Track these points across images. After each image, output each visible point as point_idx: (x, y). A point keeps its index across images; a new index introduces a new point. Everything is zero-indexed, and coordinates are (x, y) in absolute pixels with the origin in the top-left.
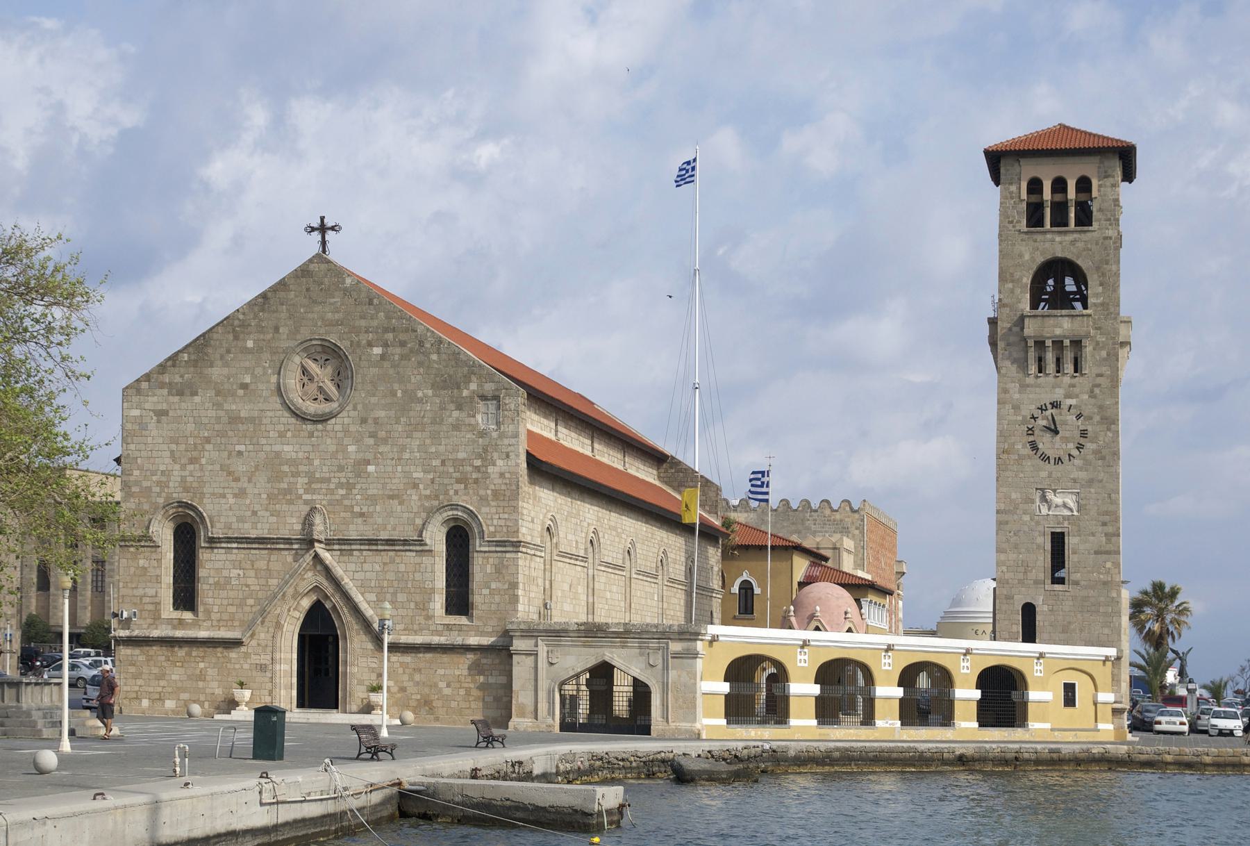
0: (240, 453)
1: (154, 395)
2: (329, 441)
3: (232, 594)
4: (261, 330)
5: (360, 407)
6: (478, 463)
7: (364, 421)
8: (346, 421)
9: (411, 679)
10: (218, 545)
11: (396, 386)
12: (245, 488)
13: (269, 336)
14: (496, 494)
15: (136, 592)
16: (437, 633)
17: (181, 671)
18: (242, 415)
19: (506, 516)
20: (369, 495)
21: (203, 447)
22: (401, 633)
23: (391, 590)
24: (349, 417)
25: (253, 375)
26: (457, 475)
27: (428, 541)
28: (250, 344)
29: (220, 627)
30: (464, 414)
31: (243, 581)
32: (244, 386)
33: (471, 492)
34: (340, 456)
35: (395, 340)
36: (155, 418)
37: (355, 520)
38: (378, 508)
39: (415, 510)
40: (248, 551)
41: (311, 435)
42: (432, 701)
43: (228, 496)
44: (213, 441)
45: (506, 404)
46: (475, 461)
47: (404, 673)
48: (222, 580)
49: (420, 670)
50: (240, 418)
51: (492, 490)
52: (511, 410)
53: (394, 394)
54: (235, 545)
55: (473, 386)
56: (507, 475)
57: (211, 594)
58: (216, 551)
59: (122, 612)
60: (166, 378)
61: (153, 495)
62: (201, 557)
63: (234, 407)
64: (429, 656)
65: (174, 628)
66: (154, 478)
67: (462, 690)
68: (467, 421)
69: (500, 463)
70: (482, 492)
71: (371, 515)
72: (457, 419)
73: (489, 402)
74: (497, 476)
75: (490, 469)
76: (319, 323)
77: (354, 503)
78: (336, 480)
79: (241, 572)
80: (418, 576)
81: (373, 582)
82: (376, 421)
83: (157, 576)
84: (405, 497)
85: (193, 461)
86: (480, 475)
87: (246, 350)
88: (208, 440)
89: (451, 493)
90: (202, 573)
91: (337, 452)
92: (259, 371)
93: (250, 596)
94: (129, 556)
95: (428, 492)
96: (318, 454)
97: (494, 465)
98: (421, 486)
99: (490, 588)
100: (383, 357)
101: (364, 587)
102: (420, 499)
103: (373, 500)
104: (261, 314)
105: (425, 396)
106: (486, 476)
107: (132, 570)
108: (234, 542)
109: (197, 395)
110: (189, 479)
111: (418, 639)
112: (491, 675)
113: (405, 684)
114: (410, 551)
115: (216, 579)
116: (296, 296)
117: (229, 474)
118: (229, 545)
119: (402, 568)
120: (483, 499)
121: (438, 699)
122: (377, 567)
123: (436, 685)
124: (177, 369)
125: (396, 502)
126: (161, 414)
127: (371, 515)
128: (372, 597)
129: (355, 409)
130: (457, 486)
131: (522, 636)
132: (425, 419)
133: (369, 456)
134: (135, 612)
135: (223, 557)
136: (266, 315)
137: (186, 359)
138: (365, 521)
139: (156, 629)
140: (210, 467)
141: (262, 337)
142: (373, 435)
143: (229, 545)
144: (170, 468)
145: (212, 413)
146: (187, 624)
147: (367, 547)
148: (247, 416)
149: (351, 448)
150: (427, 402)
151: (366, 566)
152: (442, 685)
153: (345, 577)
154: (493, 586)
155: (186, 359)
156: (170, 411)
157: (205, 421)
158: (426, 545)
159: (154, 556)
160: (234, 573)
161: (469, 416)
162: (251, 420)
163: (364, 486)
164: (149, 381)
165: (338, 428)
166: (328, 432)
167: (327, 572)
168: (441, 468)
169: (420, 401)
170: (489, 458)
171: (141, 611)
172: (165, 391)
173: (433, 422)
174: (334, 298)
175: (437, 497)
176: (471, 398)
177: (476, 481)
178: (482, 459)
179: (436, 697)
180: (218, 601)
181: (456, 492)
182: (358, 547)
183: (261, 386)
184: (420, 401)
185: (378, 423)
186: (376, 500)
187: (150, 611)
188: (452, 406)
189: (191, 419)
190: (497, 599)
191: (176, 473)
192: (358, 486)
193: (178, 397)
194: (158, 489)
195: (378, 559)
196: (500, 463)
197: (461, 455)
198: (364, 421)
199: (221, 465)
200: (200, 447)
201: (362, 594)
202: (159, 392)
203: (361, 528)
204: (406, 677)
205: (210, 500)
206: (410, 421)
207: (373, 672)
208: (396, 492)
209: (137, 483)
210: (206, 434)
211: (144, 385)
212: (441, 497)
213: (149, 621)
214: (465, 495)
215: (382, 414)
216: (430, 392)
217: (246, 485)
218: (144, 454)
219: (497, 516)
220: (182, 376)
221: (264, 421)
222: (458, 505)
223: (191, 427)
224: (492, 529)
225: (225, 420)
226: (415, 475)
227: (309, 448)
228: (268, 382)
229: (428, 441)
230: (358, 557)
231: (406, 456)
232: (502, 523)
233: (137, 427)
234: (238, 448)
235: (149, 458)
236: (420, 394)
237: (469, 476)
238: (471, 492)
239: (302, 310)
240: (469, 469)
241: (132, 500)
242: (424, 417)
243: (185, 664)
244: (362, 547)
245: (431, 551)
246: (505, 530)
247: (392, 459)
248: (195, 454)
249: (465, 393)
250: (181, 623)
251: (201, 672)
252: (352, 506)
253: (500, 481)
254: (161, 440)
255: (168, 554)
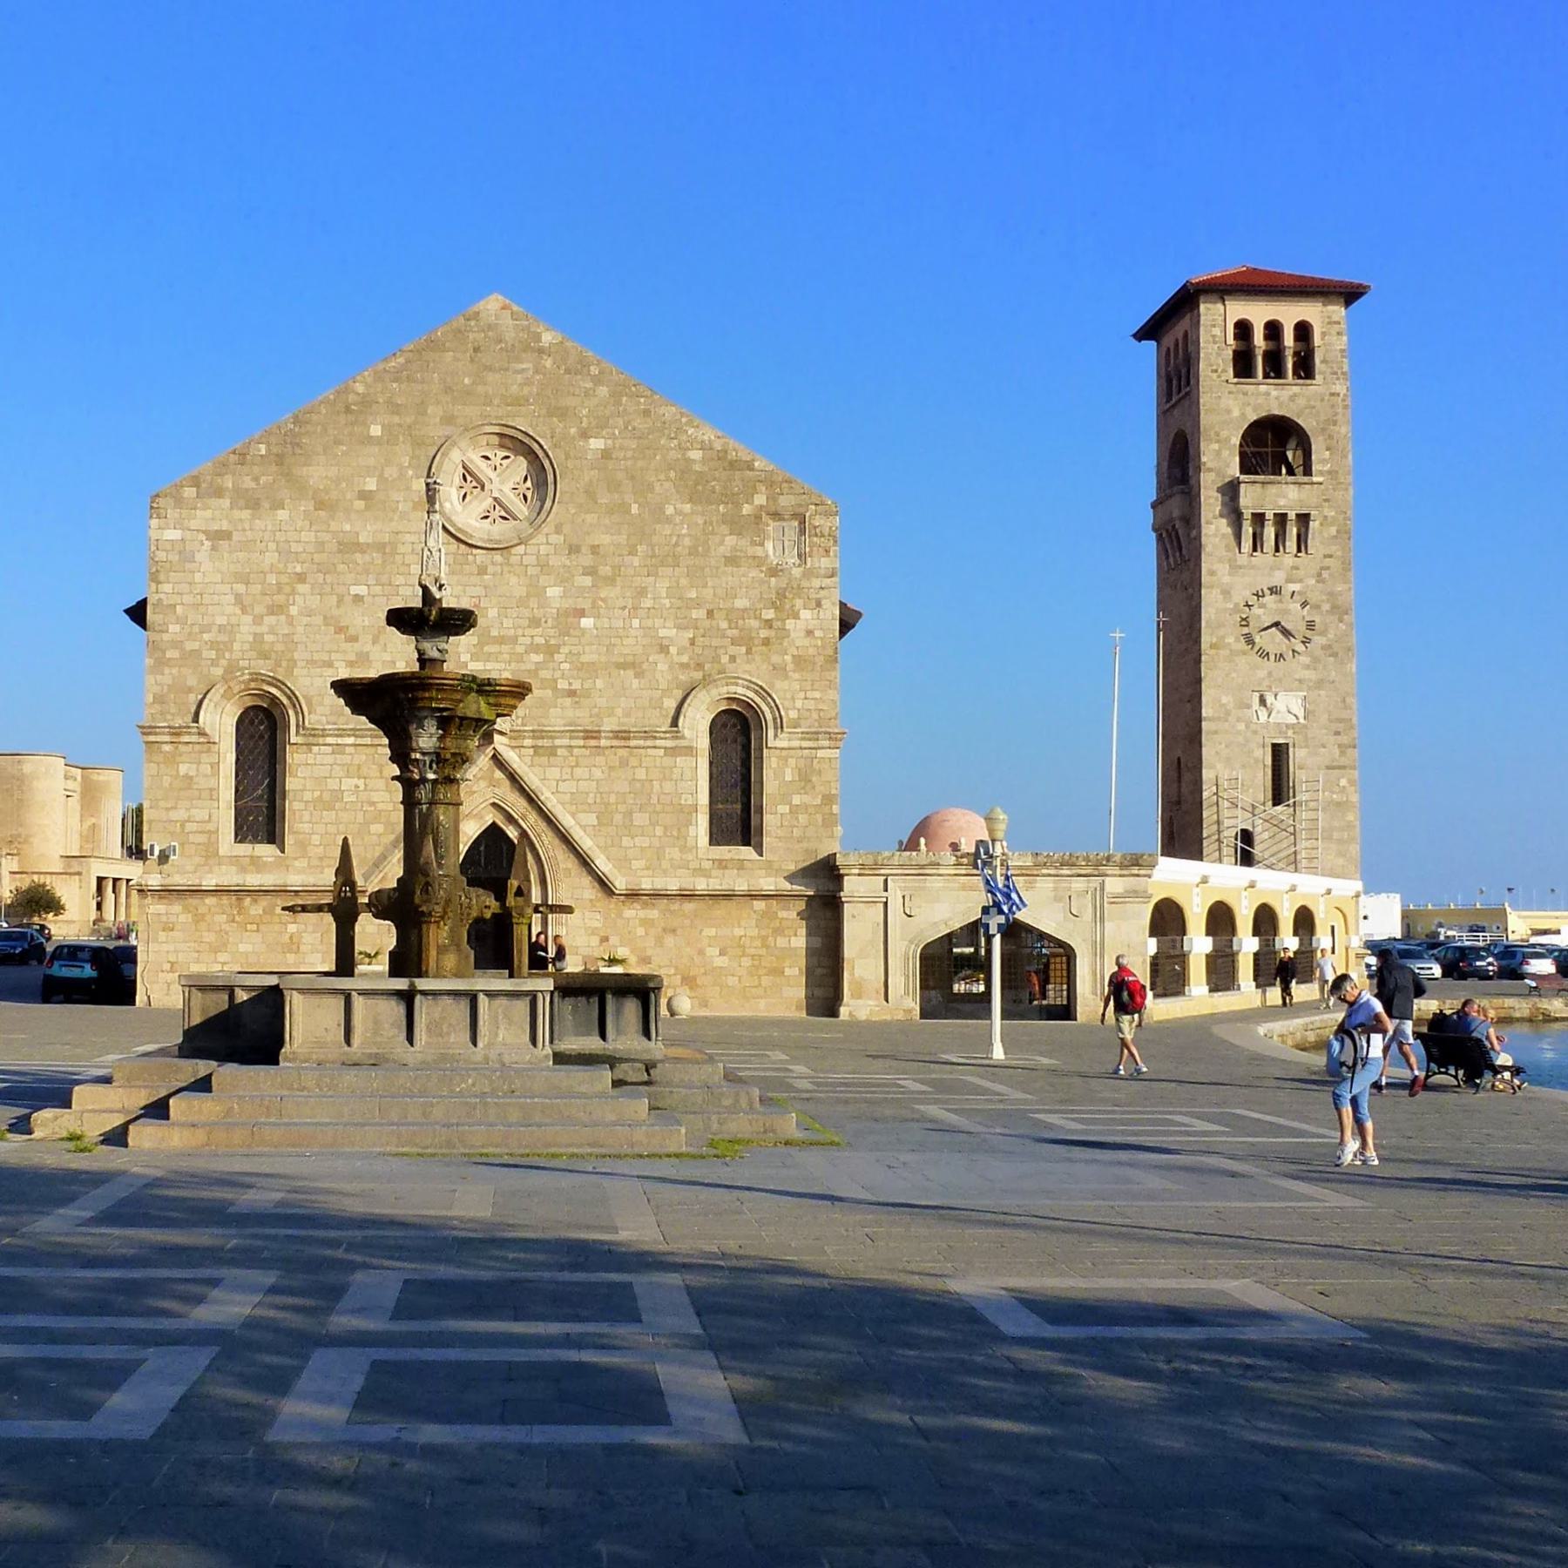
0: (358, 599)
1: (205, 508)
2: (514, 580)
3: (345, 816)
4: (396, 409)
5: (566, 529)
6: (769, 614)
7: (574, 549)
8: (543, 549)
9: (659, 942)
10: (321, 740)
11: (629, 498)
12: (368, 653)
13: (409, 420)
14: (799, 661)
15: (174, 815)
16: (701, 872)
17: (257, 938)
18: (361, 540)
19: (817, 695)
20: (582, 663)
21: (293, 589)
22: (640, 873)
23: (621, 808)
24: (548, 543)
25: (382, 479)
26: (735, 632)
27: (687, 733)
28: (376, 430)
29: (323, 868)
30: (744, 543)
31: (364, 796)
32: (364, 495)
33: (758, 658)
34: (533, 603)
35: (626, 428)
36: (206, 542)
37: (560, 701)
38: (599, 683)
39: (663, 686)
40: (372, 750)
41: (482, 571)
42: (694, 978)
43: (336, 664)
44: (310, 579)
45: (815, 527)
46: (764, 611)
47: (647, 934)
48: (326, 796)
49: (674, 931)
50: (358, 544)
51: (793, 656)
52: (823, 536)
53: (624, 508)
54: (351, 740)
55: (760, 500)
56: (818, 633)
57: (306, 817)
58: (315, 749)
59: (152, 846)
60: (228, 482)
61: (203, 663)
62: (289, 760)
63: (347, 527)
64: (689, 906)
65: (243, 870)
66: (206, 637)
67: (745, 959)
68: (751, 551)
69: (805, 614)
70: (776, 659)
71: (587, 694)
72: (734, 549)
73: (784, 524)
74: (803, 634)
75: (790, 624)
76: (496, 402)
77: (558, 674)
78: (528, 640)
79: (361, 783)
80: (668, 787)
81: (591, 795)
82: (595, 549)
83: (211, 790)
84: (645, 666)
85: (275, 610)
86: (772, 633)
87: (370, 440)
88: (301, 578)
89: (725, 659)
90: (291, 784)
91: (528, 596)
92: (391, 472)
93: (376, 820)
94: (160, 758)
95: (685, 659)
96: (494, 601)
97: (796, 616)
98: (673, 650)
99: (791, 804)
100: (606, 454)
101: (577, 803)
102: (671, 668)
103: (590, 670)
104: (395, 385)
105: (678, 512)
106: (784, 634)
107: (166, 781)
108: (349, 736)
109: (283, 509)
110: (266, 637)
111: (673, 885)
112: (796, 935)
113: (649, 952)
114: (655, 747)
115: (317, 794)
116: (456, 359)
117: (340, 630)
118: (340, 741)
119: (641, 774)
120: (779, 671)
121: (705, 974)
122: (598, 773)
123: (701, 952)
124: (246, 469)
125: (630, 673)
126: (218, 537)
127: (587, 694)
128: (592, 819)
129: (558, 530)
130: (733, 650)
131: (859, 875)
132: (679, 549)
133: (586, 605)
134: (174, 846)
135: (329, 759)
136: (403, 386)
137: (263, 452)
138: (576, 702)
139: (211, 871)
140: (305, 620)
141: (396, 419)
142: (590, 571)
143: (340, 741)
144: (234, 620)
145: (309, 536)
146: (265, 864)
147: (581, 743)
148: (370, 541)
149: (551, 592)
150: (682, 523)
151: (578, 772)
152: (713, 952)
153: (544, 789)
154: (796, 800)
155: (263, 452)
156: (234, 533)
157: (294, 547)
158: (683, 737)
159: (205, 758)
160: (347, 784)
161: (753, 543)
162: (381, 547)
163: (575, 650)
164: (197, 486)
165: (526, 560)
166: (512, 565)
167: (513, 778)
168: (707, 623)
169: (669, 520)
170: (787, 607)
171: (182, 845)
172: (226, 503)
173: (693, 552)
174: (522, 363)
175: (700, 666)
176: (758, 518)
177: (766, 642)
178: (776, 608)
179: (702, 970)
180: (320, 828)
181: (733, 659)
182: (566, 742)
183: (395, 496)
184: (669, 520)
185: (598, 554)
186: (596, 671)
187: (199, 844)
188: (725, 529)
189: (272, 546)
190: (803, 819)
191: (244, 629)
192: (564, 650)
193: (249, 511)
194: (213, 654)
195: (600, 760)
196: (805, 614)
197: (740, 603)
198: (574, 549)
199: (325, 618)
200: (287, 589)
201: (573, 815)
202: (214, 502)
203: (570, 713)
204: (650, 942)
205: (305, 672)
206: (653, 550)
207: (593, 934)
208: (630, 659)
209: (176, 644)
210: (298, 569)
211: (189, 492)
212: (707, 666)
213: (197, 860)
214: (748, 662)
215: (604, 539)
216: (687, 507)
217: (368, 648)
218: (187, 599)
219: (802, 695)
220: (256, 479)
221: (401, 549)
222: (738, 678)
223: (271, 558)
224: (793, 714)
225: (333, 546)
226: (662, 633)
227: (479, 591)
228: (408, 488)
229: (684, 582)
230: (565, 758)
231: (647, 603)
232: (811, 705)
233: (177, 557)
234: (354, 590)
235: (196, 606)
236: (670, 510)
237: (753, 635)
238: (758, 658)
239: (466, 381)
240: (754, 623)
241: (167, 671)
242: (676, 544)
243: (262, 927)
244: (574, 743)
245: (690, 748)
246: (815, 716)
247: (624, 608)
248: (280, 599)
249: (747, 509)
250: (256, 864)
251: (291, 938)
252: (555, 681)
253: (806, 642)
254: (218, 578)
255: (228, 755)
